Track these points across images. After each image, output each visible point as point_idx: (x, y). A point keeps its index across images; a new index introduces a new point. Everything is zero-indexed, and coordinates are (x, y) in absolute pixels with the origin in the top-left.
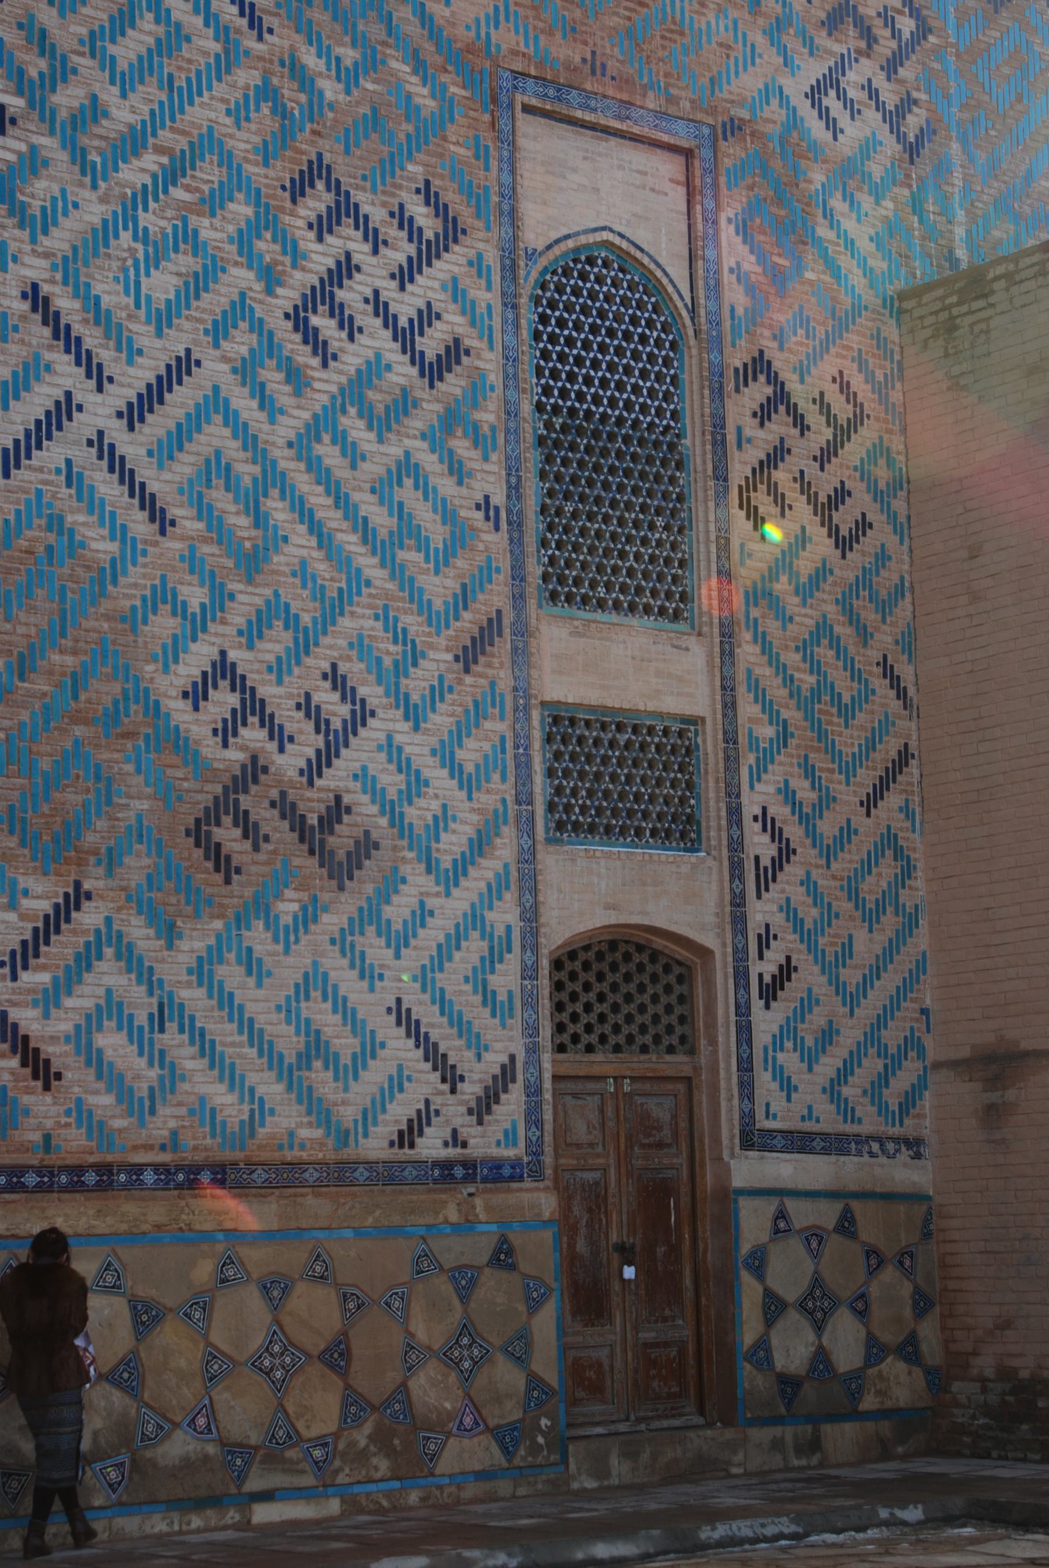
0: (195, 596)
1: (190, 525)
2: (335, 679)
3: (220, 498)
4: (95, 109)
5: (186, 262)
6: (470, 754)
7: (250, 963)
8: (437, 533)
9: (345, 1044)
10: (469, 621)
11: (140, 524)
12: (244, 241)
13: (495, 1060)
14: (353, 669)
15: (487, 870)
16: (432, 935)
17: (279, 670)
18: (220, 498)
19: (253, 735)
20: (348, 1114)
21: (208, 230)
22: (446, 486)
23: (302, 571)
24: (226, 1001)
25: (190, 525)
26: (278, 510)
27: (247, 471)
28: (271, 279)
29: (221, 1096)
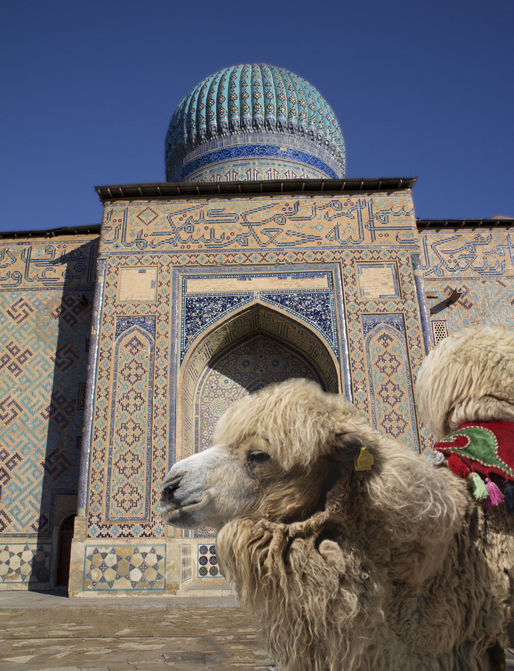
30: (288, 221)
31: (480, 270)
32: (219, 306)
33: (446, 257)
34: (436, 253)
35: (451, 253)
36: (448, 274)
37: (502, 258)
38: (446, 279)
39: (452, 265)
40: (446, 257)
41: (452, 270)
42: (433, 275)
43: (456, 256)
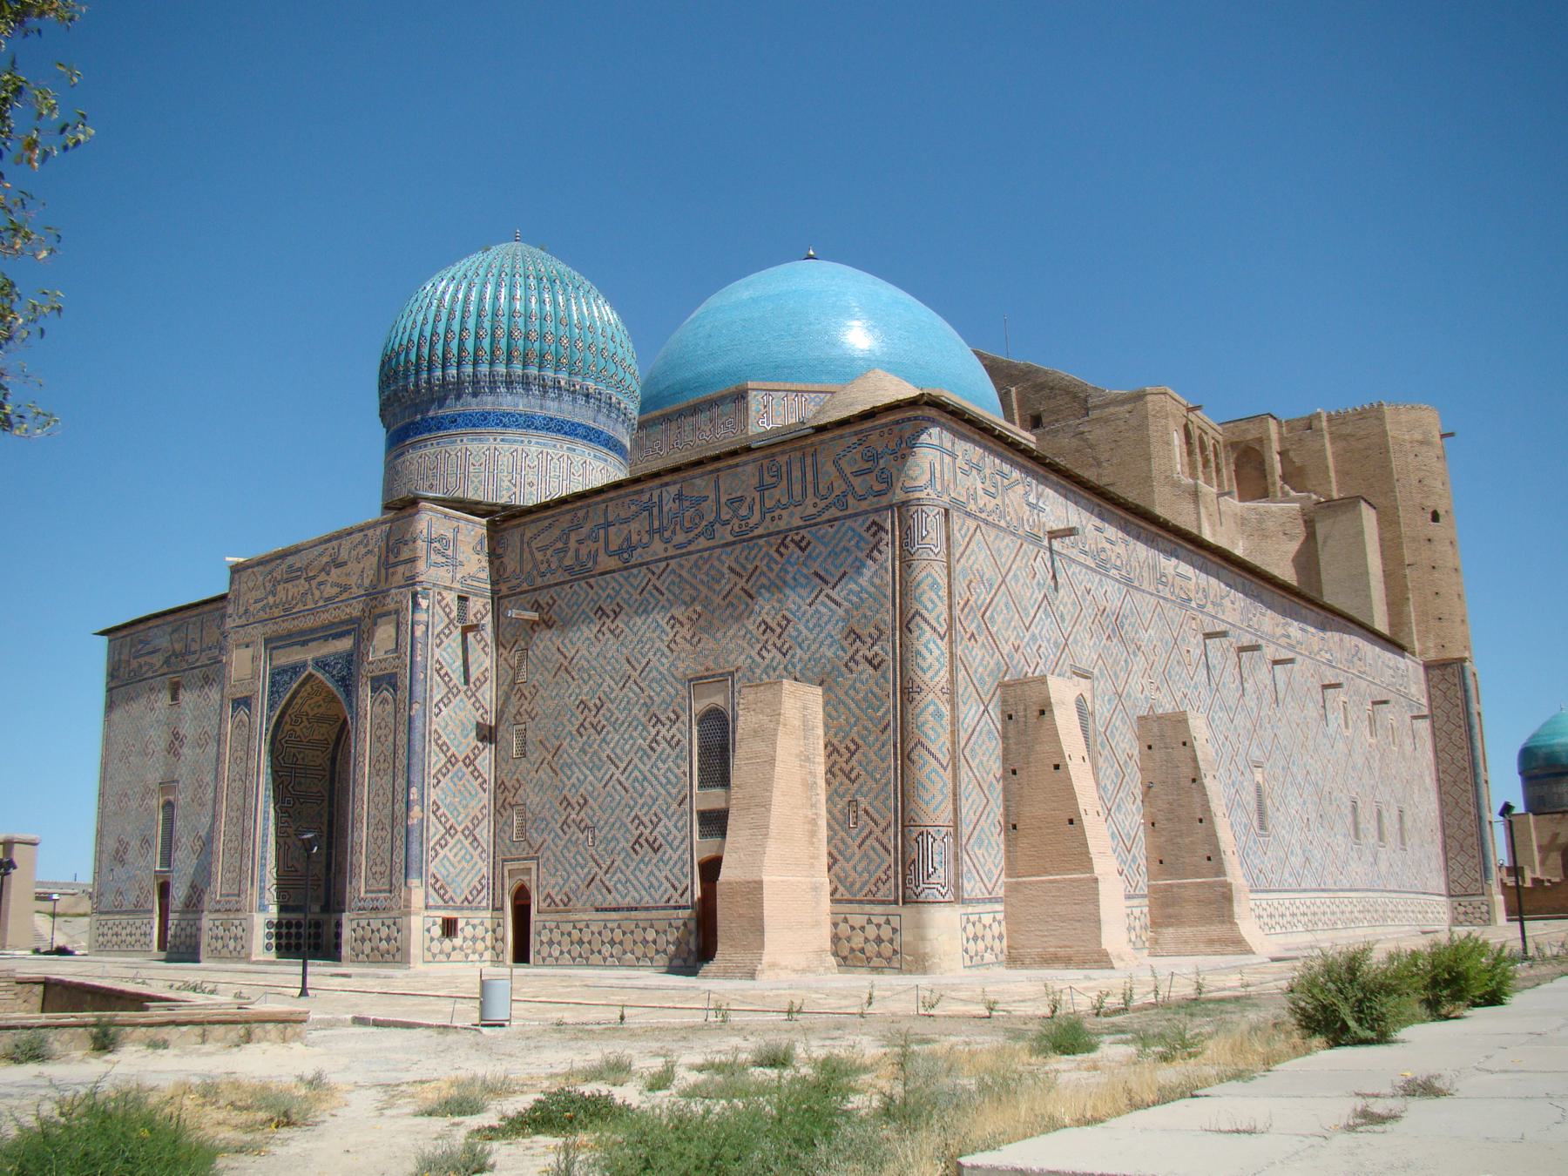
0: (632, 803)
1: (631, 790)
2: (656, 815)
3: (636, 784)
4: (617, 719)
5: (631, 742)
6: (680, 824)
7: (641, 871)
8: (674, 780)
9: (656, 884)
10: (680, 797)
11: (623, 792)
12: (640, 735)
13: (684, 886)
14: (659, 811)
15: (683, 846)
16: (671, 863)
17: (645, 815)
18: (636, 784)
19: (641, 827)
20: (657, 897)
21: (635, 734)
22: (676, 771)
23: (650, 795)
24: (636, 877)
25: (631, 790)
26: (646, 784)
27: (641, 778)
28: (645, 740)
29: (636, 895)
30: (333, 571)
31: (569, 569)
32: (286, 678)
33: (539, 556)
34: (532, 554)
35: (543, 549)
36: (539, 582)
37: (596, 545)
38: (535, 590)
39: (543, 568)
40: (539, 556)
41: (543, 575)
42: (525, 586)
43: (549, 552)
